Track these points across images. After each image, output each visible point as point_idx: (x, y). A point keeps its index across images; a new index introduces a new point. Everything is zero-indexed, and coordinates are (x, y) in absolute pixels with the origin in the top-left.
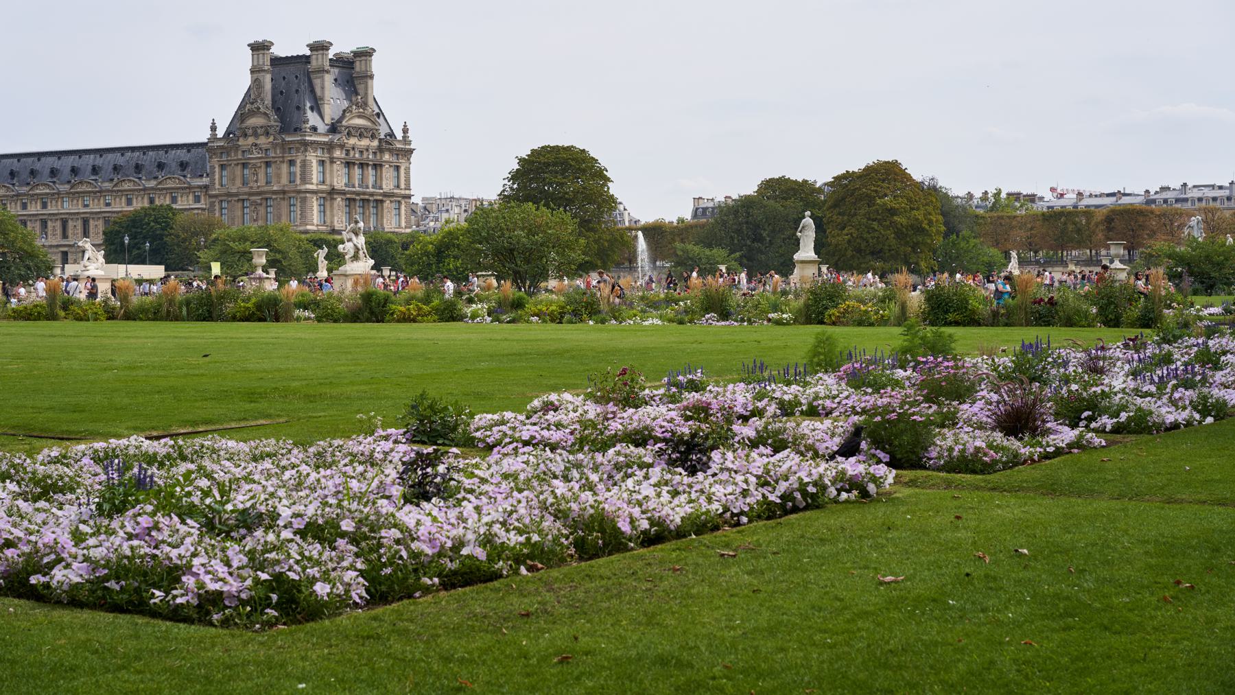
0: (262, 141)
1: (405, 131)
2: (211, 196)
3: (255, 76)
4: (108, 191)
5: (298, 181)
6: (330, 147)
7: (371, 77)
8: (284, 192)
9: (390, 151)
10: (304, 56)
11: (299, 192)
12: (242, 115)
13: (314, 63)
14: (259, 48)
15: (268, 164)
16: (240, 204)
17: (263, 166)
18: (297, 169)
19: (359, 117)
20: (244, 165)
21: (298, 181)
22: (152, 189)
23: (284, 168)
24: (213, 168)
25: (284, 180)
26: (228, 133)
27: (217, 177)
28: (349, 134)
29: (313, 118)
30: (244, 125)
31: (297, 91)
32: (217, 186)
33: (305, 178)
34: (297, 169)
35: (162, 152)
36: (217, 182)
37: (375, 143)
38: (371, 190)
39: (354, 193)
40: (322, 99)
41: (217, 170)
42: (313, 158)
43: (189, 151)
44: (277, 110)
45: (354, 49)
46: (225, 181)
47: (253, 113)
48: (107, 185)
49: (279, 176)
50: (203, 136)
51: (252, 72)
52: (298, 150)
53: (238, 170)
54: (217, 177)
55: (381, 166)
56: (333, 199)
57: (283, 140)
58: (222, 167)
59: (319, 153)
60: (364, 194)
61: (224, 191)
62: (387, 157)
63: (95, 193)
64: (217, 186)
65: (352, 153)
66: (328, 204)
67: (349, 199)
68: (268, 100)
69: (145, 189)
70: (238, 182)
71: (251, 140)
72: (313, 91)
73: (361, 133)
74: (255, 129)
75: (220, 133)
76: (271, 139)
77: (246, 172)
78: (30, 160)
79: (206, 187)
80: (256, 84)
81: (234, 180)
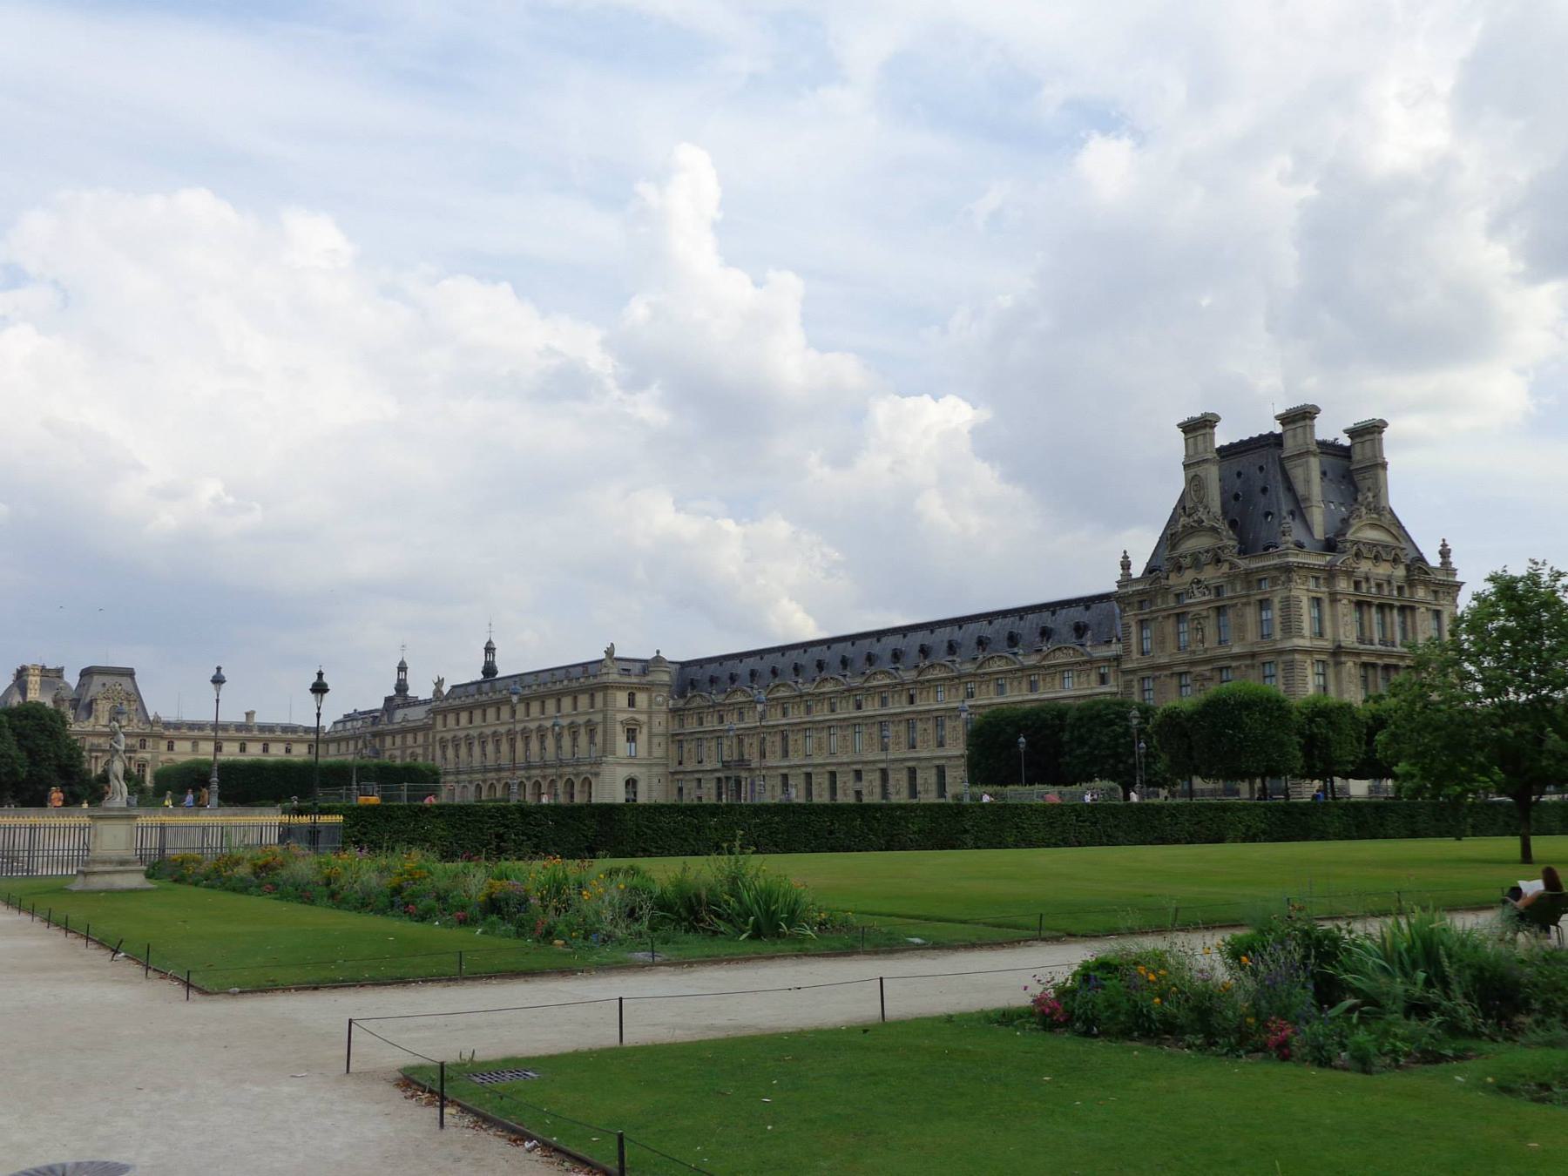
0: (1210, 574)
1: (1445, 553)
2: (1125, 672)
3: (1192, 472)
4: (970, 675)
5: (1278, 635)
6: (1330, 574)
7: (1384, 466)
8: (1253, 655)
9: (1426, 583)
10: (1271, 434)
11: (1281, 652)
12: (1171, 538)
13: (1290, 446)
14: (1196, 428)
15: (1220, 610)
16: (1175, 681)
17: (1213, 614)
18: (1275, 614)
19: (1373, 526)
20: (1180, 617)
21: (1278, 635)
22: (1035, 667)
23: (1251, 614)
24: (1127, 626)
25: (1252, 635)
26: (1150, 569)
27: (1134, 640)
28: (1358, 555)
29: (1297, 532)
30: (1175, 554)
31: (1264, 490)
32: (1135, 655)
33: (1289, 627)
34: (1275, 614)
35: (1046, 614)
36: (1134, 648)
37: (1401, 572)
38: (1399, 649)
40: (1307, 499)
43: (1087, 608)
44: (1233, 524)
46: (1147, 645)
47: (1190, 531)
48: (969, 668)
49: (1241, 628)
50: (1107, 582)
51: (1186, 466)
52: (1274, 581)
53: (1169, 626)
54: (1134, 640)
55: (1413, 609)
56: (1338, 664)
58: (1142, 624)
59: (1312, 584)
60: (1390, 656)
61: (1146, 662)
62: (1421, 593)
63: (952, 679)
64: (1135, 655)
65: (1364, 586)
66: (1331, 672)
67: (1365, 665)
68: (1216, 506)
69: (1022, 669)
70: (1170, 646)
71: (1189, 575)
72: (1290, 488)
73: (1377, 553)
75: (1137, 570)
76: (1225, 568)
77: (1183, 627)
78: (867, 642)
79: (1117, 658)
80: (1194, 484)
81: (1163, 642)
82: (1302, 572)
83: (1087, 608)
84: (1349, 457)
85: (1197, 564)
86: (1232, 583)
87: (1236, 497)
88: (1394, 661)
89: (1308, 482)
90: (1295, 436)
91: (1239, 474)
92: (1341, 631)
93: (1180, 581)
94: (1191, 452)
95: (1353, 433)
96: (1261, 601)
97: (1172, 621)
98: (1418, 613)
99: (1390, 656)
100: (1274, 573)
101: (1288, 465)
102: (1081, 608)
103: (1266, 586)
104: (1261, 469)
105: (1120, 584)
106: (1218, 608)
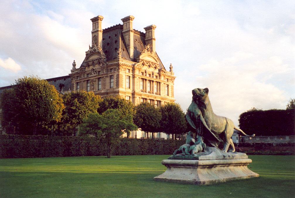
0: (97, 67)
17: (97, 80)
23: (108, 80)
25: (108, 87)
34: (114, 80)
39: (145, 95)
41: (75, 85)
42: (124, 74)
43: (65, 80)
45: (146, 27)
51: (92, 33)
52: (115, 69)
57: (107, 65)
71: (91, 67)
74: (93, 61)
75: (78, 66)
80: (95, 39)
82: (124, 67)
83: (65, 80)
84: (145, 37)
85: (93, 64)
86: (103, 70)
87: (108, 44)
88: (152, 98)
89: (129, 40)
90: (126, 25)
91: (110, 37)
92: (136, 87)
93: (89, 69)
94: (94, 28)
95: (146, 29)
96: (111, 76)
97: (85, 82)
98: (161, 84)
99: (151, 97)
100: (115, 67)
101: (124, 35)
102: (63, 80)
103: (113, 71)
104: (116, 35)
105: (72, 71)
106: (99, 78)
